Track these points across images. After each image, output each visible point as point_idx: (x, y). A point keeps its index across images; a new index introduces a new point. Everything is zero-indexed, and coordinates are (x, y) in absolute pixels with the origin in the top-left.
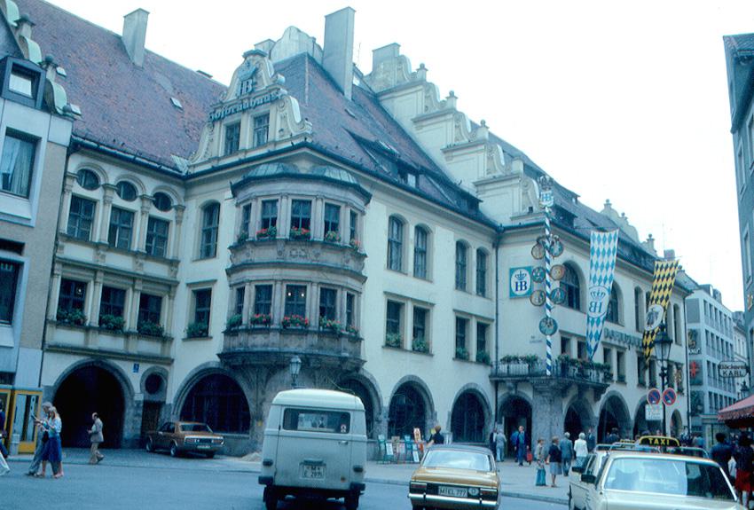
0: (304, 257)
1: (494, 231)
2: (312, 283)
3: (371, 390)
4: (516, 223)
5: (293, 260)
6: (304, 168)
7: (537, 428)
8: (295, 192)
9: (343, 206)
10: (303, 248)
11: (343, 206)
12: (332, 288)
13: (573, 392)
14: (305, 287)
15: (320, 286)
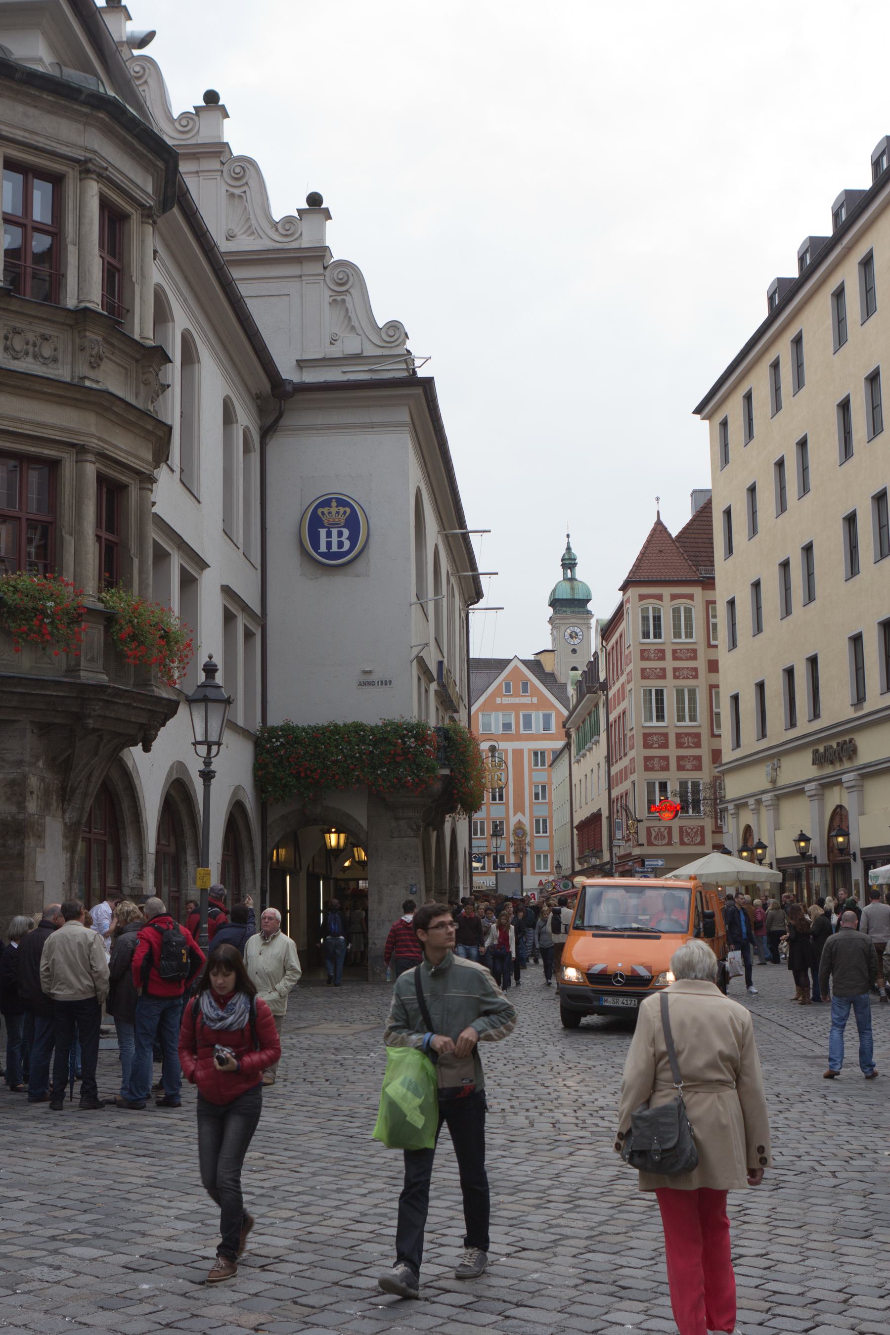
0: (45, 361)
1: (267, 387)
2: (81, 450)
3: (125, 804)
4: (311, 377)
5: (20, 366)
6: (40, 60)
7: (380, 902)
8: (19, 135)
9: (135, 217)
10: (47, 330)
11: (135, 217)
12: (124, 478)
14: (54, 465)
15: (97, 465)
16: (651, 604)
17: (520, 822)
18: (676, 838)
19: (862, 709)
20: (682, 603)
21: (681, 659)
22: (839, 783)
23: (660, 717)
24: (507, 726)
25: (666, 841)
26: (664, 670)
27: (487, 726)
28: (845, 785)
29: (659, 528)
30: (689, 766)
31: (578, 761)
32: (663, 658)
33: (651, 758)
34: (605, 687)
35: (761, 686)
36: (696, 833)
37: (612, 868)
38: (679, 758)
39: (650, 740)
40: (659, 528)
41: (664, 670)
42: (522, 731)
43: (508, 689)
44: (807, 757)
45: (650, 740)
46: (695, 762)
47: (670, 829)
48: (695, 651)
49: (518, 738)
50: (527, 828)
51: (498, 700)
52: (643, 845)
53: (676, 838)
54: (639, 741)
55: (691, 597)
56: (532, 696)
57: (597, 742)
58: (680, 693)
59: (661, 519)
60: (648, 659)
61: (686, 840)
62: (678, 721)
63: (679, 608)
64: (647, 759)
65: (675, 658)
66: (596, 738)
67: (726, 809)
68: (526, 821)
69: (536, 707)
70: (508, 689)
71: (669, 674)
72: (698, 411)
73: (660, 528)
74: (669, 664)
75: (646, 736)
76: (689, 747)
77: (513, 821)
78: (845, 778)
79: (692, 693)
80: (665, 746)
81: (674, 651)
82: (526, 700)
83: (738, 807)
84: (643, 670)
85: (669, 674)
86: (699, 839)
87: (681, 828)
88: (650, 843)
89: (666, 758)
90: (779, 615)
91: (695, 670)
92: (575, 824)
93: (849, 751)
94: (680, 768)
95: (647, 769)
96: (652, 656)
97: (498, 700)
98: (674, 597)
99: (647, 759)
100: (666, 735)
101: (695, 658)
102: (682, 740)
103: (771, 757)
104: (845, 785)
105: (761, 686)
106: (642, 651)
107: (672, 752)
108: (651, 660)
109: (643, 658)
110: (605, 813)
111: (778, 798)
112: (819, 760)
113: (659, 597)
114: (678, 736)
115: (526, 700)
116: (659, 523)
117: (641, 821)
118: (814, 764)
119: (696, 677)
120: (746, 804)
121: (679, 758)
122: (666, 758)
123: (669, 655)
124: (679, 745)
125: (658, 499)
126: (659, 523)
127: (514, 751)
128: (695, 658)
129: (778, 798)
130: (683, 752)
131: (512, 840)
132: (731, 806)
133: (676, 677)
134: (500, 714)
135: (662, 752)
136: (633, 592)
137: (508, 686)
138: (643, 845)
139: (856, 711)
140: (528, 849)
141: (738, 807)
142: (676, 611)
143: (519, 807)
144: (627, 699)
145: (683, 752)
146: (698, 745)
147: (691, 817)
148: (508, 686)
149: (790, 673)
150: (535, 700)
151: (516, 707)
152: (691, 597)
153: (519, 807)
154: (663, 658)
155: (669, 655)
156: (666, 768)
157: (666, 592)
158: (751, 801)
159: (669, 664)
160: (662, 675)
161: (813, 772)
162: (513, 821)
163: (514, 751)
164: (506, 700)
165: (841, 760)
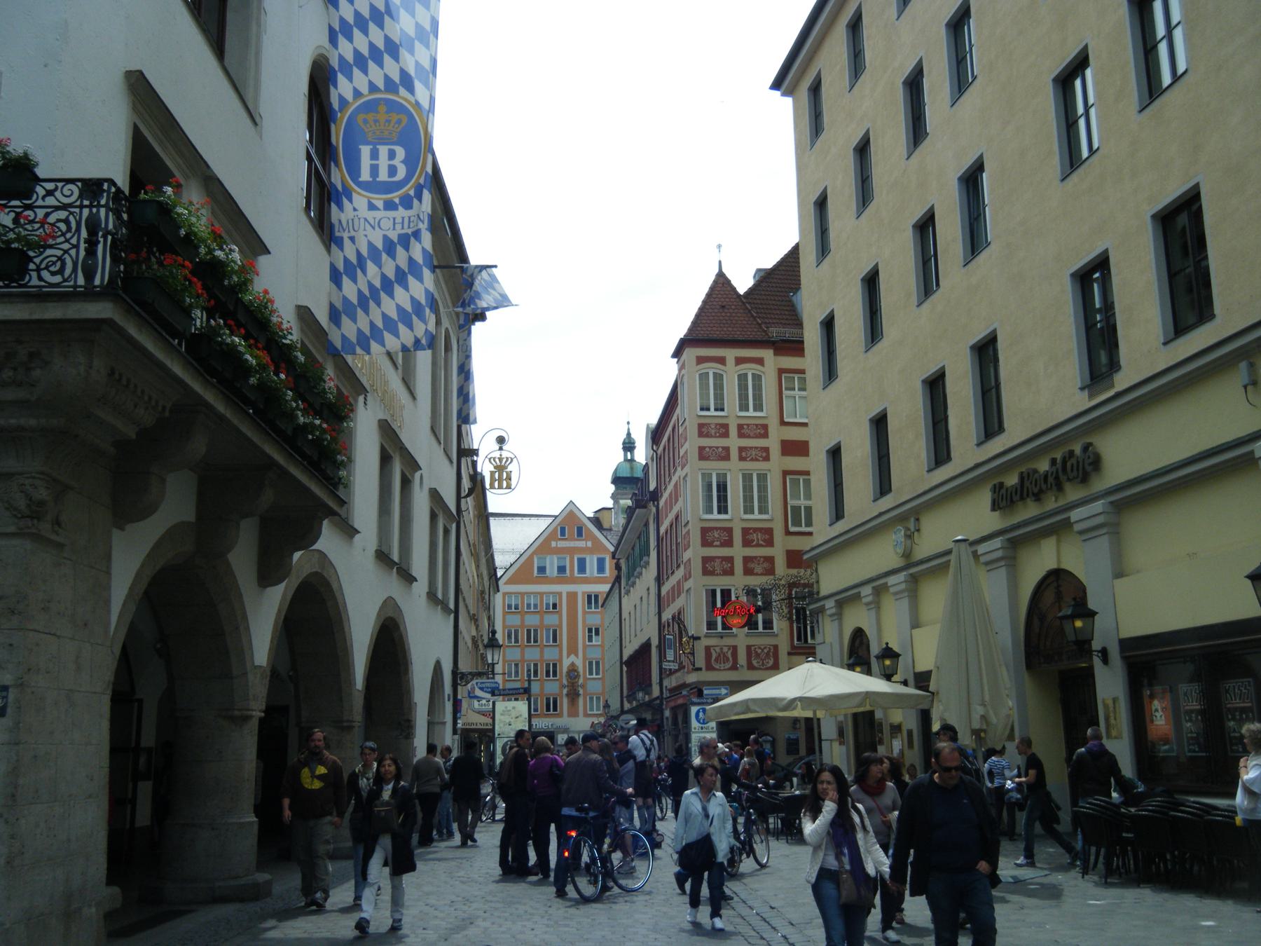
13: (175, 504)
16: (711, 369)
17: (573, 664)
18: (742, 659)
19: (1112, 386)
20: (750, 369)
21: (749, 437)
22: (1067, 525)
23: (723, 509)
24: (562, 569)
25: (728, 665)
26: (727, 449)
27: (542, 569)
28: (1077, 527)
29: (722, 283)
30: (758, 569)
31: (628, 592)
32: (726, 435)
33: (712, 559)
34: (655, 496)
35: (880, 423)
36: (768, 654)
37: (662, 703)
38: (746, 560)
39: (710, 537)
40: (722, 283)
41: (727, 449)
42: (576, 574)
43: (563, 533)
44: (984, 497)
45: (710, 537)
46: (766, 565)
47: (734, 649)
48: (765, 427)
49: (573, 581)
50: (581, 670)
51: (553, 544)
52: (700, 669)
53: (742, 659)
54: (696, 538)
55: (760, 361)
56: (586, 540)
57: (648, 563)
58: (747, 478)
59: (724, 270)
60: (708, 435)
61: (755, 663)
62: (745, 513)
63: (746, 375)
64: (706, 560)
65: (741, 435)
66: (645, 558)
67: (822, 610)
68: (579, 662)
69: (591, 551)
70: (563, 533)
71: (734, 454)
72: (777, 85)
73: (721, 280)
74: (734, 442)
75: (705, 531)
76: (758, 545)
77: (566, 663)
78: (1075, 515)
79: (762, 478)
80: (729, 543)
81: (740, 427)
82: (581, 544)
83: (840, 605)
84: (701, 449)
85: (734, 454)
86: (771, 662)
87: (749, 648)
88: (709, 667)
89: (730, 560)
90: (914, 300)
91: (766, 450)
92: (625, 658)
93: (1085, 466)
94: (748, 572)
95: (706, 572)
96: (713, 432)
97: (553, 544)
98: (739, 361)
99: (706, 560)
100: (729, 531)
101: (765, 435)
102: (750, 537)
103: (902, 519)
104: (1077, 527)
105: (880, 423)
106: (701, 426)
107: (738, 552)
108: (711, 436)
109: (701, 434)
110: (655, 642)
111: (914, 580)
112: (1004, 500)
113: (722, 361)
114: (745, 531)
115: (581, 544)
116: (721, 276)
117: (699, 638)
118: (993, 509)
119: (767, 459)
120: (857, 597)
121: (746, 560)
122: (730, 560)
123: (733, 431)
124: (747, 543)
125: (719, 246)
126: (721, 276)
127: (569, 594)
128: (765, 435)
129: (914, 580)
130: (751, 552)
131: (565, 682)
132: (830, 604)
133: (742, 459)
134: (555, 558)
135: (725, 552)
136: (691, 353)
137: (563, 530)
138: (700, 669)
139: (1091, 396)
140: (581, 692)
141: (840, 605)
142: (742, 378)
143: (573, 650)
144: (681, 500)
145: (751, 552)
146: (770, 543)
147: (761, 634)
148: (563, 530)
149: (935, 385)
150: (589, 544)
151: (571, 551)
152: (760, 361)
153: (573, 650)
154: (726, 435)
155: (733, 431)
156: (730, 572)
157: (730, 354)
158: (866, 591)
159: (734, 442)
160: (725, 455)
161: (991, 521)
162: (566, 663)
163: (569, 594)
164: (562, 544)
165: (1060, 488)
